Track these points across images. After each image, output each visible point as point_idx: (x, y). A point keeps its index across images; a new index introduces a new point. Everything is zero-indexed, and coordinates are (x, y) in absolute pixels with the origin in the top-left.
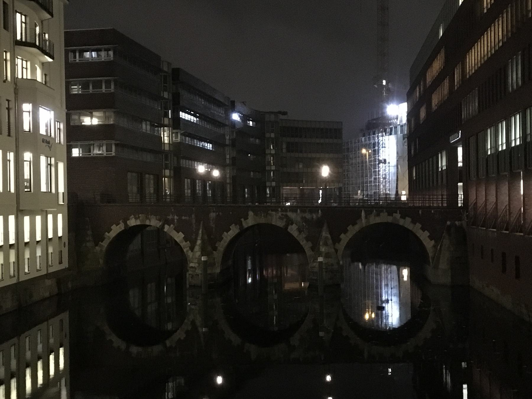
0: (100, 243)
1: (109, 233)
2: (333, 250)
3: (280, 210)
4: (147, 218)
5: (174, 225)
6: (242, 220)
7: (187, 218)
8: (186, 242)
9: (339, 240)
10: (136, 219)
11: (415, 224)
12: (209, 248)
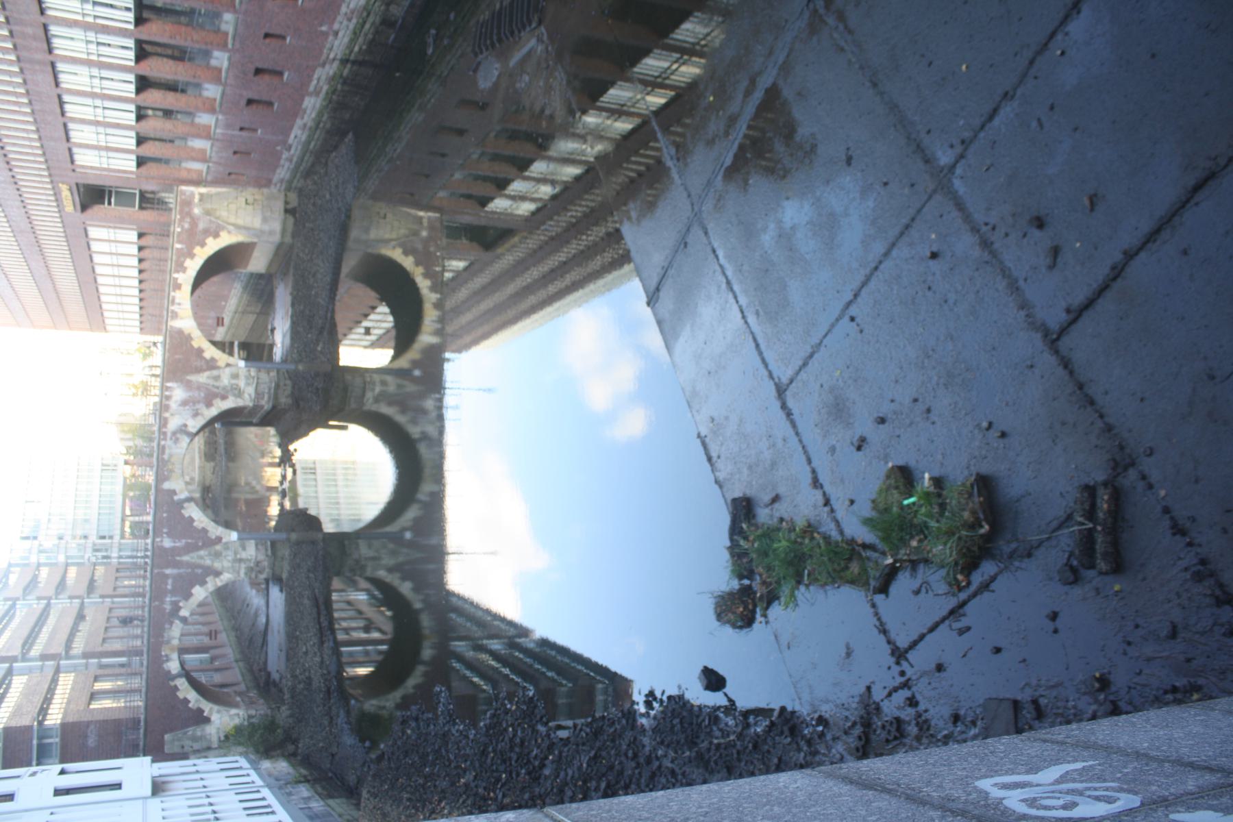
0: (205, 714)
1: (189, 702)
2: (228, 370)
3: (163, 443)
4: (168, 642)
5: (179, 601)
6: (176, 498)
7: (170, 581)
9: (213, 359)
10: (168, 660)
11: (195, 255)
12: (218, 547)
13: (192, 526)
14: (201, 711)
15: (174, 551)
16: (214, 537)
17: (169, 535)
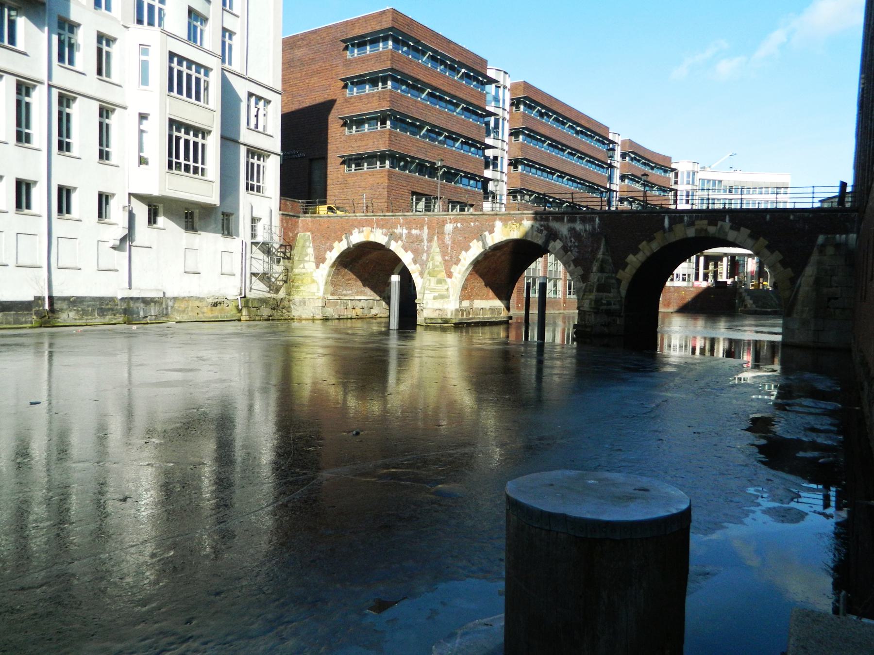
2: (613, 281)
5: (402, 241)
6: (487, 233)
8: (415, 265)
10: (359, 232)
12: (443, 275)
13: (461, 250)
14: (323, 260)
15: (441, 233)
16: (451, 270)
17: (456, 228)
